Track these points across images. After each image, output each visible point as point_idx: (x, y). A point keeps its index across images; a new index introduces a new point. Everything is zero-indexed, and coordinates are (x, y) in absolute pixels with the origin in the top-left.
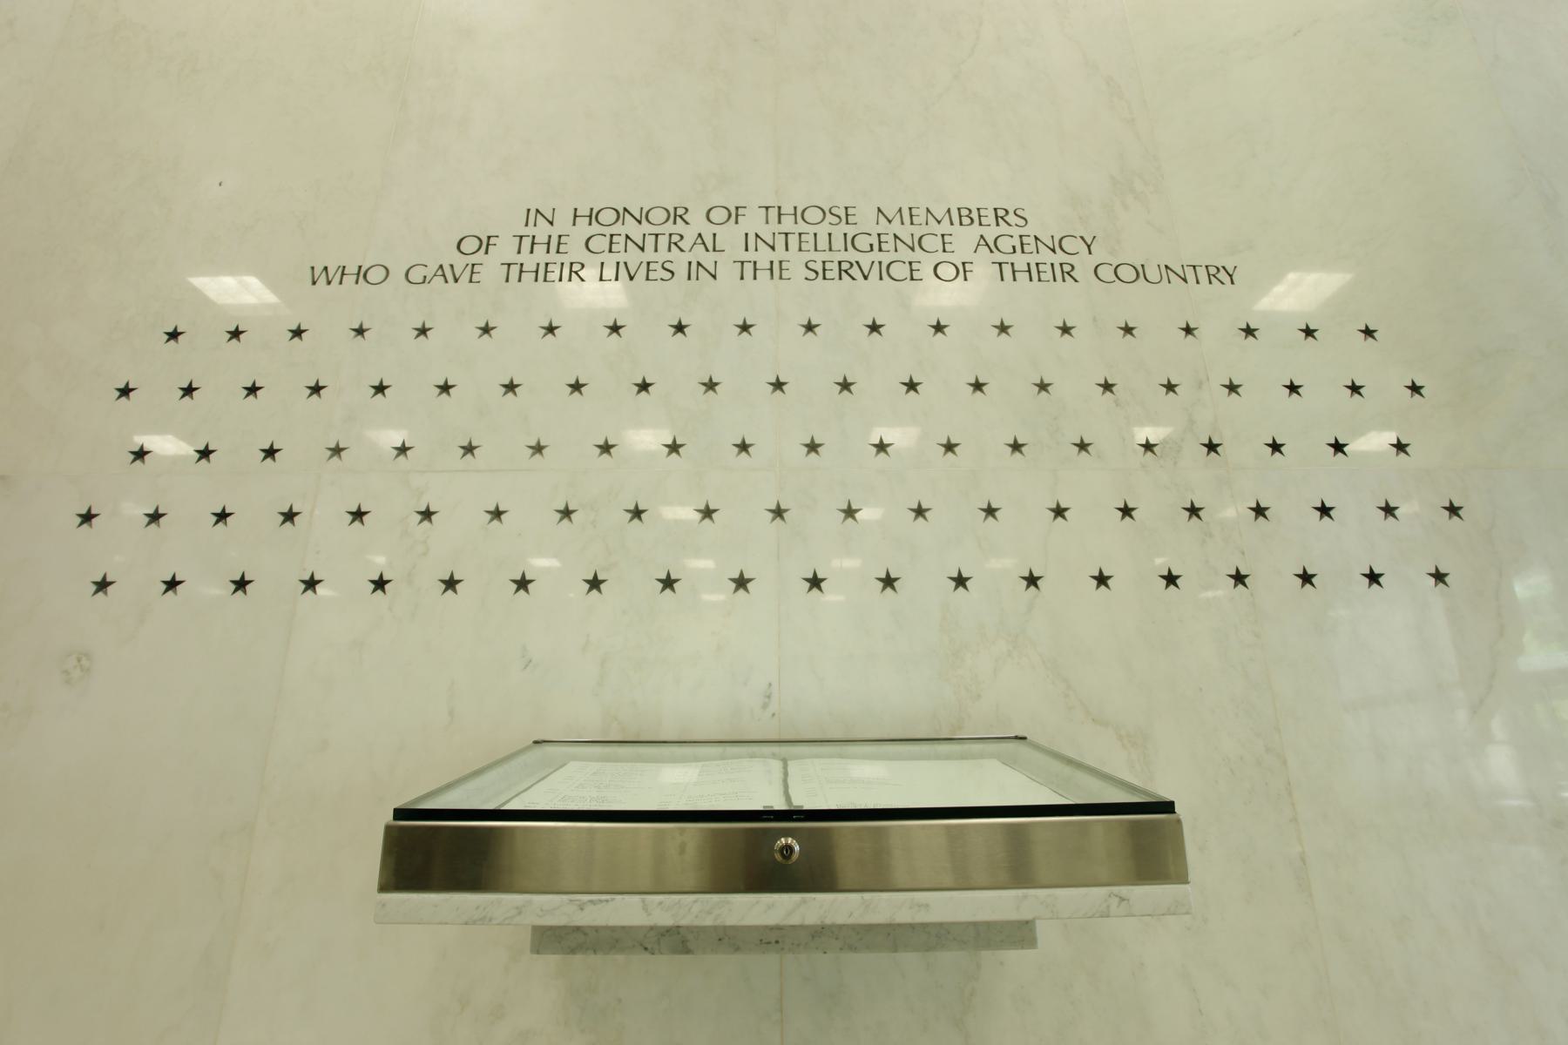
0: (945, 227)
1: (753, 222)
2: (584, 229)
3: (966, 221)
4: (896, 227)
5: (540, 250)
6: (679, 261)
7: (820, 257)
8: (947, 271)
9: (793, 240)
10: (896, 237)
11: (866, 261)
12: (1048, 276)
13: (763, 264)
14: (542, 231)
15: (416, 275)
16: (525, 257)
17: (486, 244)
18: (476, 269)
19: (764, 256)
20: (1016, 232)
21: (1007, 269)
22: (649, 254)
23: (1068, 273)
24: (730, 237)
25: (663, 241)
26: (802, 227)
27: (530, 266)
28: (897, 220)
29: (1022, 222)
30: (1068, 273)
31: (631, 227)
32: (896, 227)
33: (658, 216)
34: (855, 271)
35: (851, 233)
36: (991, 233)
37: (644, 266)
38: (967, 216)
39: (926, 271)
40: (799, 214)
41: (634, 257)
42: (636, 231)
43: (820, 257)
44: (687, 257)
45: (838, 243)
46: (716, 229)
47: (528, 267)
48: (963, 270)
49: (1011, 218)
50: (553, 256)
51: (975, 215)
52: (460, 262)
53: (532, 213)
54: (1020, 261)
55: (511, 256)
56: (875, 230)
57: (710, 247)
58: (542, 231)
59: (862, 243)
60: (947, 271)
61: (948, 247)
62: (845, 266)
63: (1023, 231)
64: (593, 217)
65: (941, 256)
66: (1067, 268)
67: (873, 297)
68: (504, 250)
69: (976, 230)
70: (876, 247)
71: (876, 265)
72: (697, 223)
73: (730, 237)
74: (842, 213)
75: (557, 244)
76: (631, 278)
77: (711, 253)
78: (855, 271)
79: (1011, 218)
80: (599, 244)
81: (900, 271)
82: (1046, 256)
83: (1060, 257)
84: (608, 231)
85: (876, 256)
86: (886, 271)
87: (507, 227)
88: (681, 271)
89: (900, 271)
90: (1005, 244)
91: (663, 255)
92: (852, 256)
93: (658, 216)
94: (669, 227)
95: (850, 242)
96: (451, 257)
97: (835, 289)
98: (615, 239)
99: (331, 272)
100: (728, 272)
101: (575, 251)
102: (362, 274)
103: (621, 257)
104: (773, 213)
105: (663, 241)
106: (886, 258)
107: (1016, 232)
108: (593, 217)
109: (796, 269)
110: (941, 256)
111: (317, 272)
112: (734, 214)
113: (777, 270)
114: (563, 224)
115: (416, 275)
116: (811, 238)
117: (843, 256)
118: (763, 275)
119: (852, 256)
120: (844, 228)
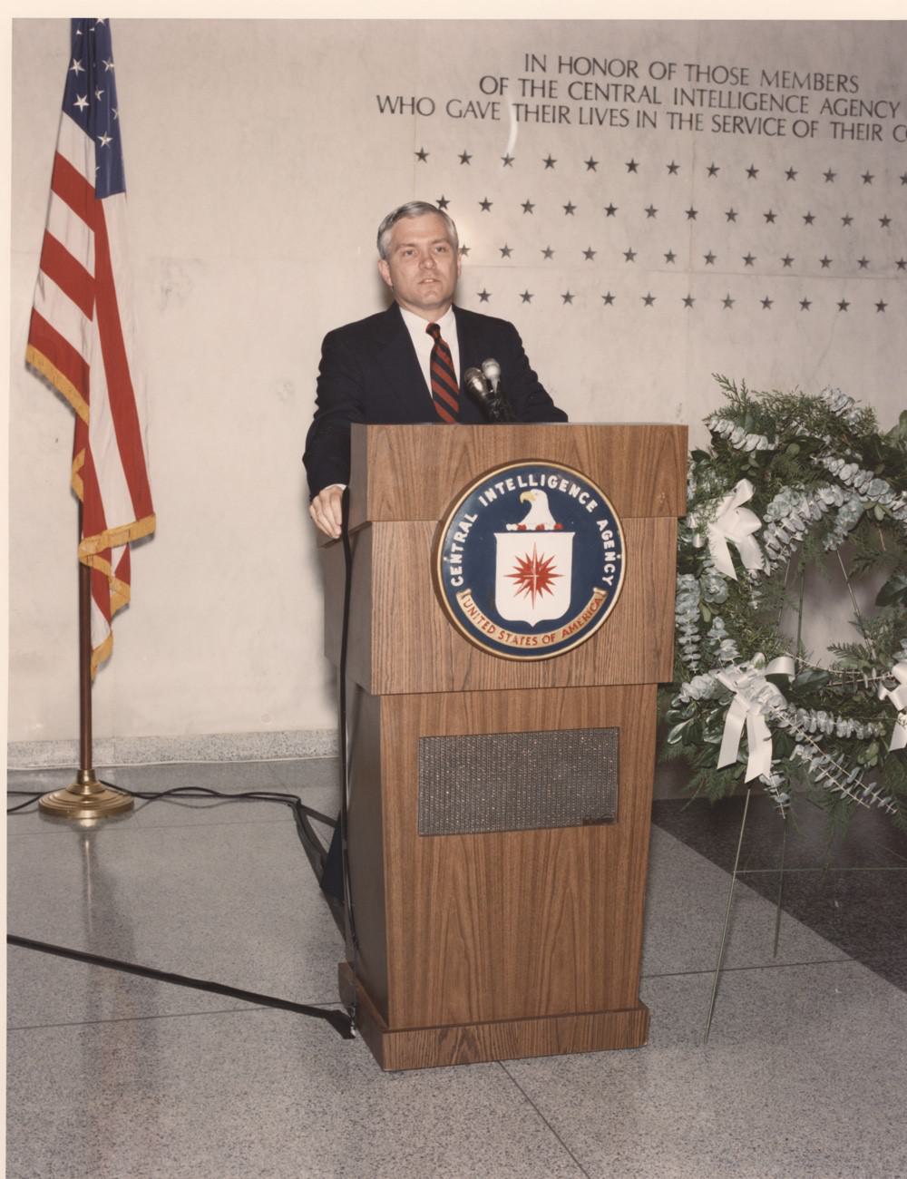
0: (804, 91)
1: (680, 80)
2: (566, 77)
3: (819, 85)
4: (773, 90)
5: (538, 92)
6: (632, 109)
7: (723, 112)
8: (801, 129)
9: (706, 95)
10: (772, 98)
11: (751, 116)
12: (863, 135)
13: (686, 117)
14: (538, 76)
15: (454, 109)
16: (527, 99)
17: (500, 86)
18: (496, 107)
19: (686, 109)
20: (849, 96)
21: (839, 128)
22: (612, 104)
23: (877, 133)
24: (665, 90)
25: (621, 90)
26: (713, 86)
27: (532, 108)
28: (774, 84)
29: (854, 88)
30: (877, 133)
32: (773, 90)
33: (617, 68)
34: (744, 126)
35: (744, 90)
36: (833, 97)
37: (609, 112)
38: (820, 81)
39: (787, 129)
40: (711, 74)
41: (602, 105)
43: (723, 112)
44: (637, 107)
45: (735, 102)
46: (656, 83)
47: (532, 108)
49: (849, 85)
50: (547, 101)
51: (825, 81)
52: (484, 100)
53: (530, 58)
54: (848, 121)
56: (759, 90)
57: (652, 98)
58: (538, 76)
59: (751, 101)
61: (805, 109)
62: (738, 121)
63: (853, 96)
64: (573, 65)
65: (799, 116)
66: (877, 129)
67: (753, 147)
68: (511, 95)
69: (824, 94)
70: (758, 107)
71: (757, 121)
72: (642, 80)
73: (665, 90)
74: (738, 73)
75: (548, 89)
76: (601, 123)
77: (653, 105)
78: (744, 126)
79: (849, 85)
81: (772, 127)
82: (867, 119)
83: (875, 120)
84: (584, 79)
85: (758, 114)
87: (514, 71)
88: (633, 119)
89: (772, 127)
90: (841, 107)
91: (620, 105)
92: (742, 112)
93: (617, 68)
94: (624, 80)
95: (743, 100)
96: (476, 95)
97: (731, 139)
98: (589, 87)
99: (393, 101)
100: (663, 121)
102: (415, 106)
103: (593, 104)
104: (694, 70)
105: (621, 90)
106: (764, 115)
107: (849, 96)
108: (573, 65)
109: (708, 124)
110: (799, 116)
111: (383, 100)
112: (668, 71)
113: (694, 122)
114: (552, 72)
115: (454, 109)
116: (716, 95)
117: (735, 112)
118: (686, 125)
119: (742, 112)
120: (740, 88)
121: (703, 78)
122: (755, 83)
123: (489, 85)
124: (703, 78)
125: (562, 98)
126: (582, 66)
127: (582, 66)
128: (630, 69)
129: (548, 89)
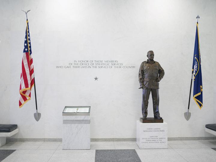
2: (79, 63)
8: (110, 67)
11: (103, 66)
14: (76, 63)
17: (71, 64)
31: (83, 63)
39: (108, 67)
42: (83, 63)
48: (111, 67)
55: (74, 65)
60: (110, 67)
80: (81, 64)
86: (105, 67)
100: (92, 67)
101: (79, 65)
108: (80, 61)
121: (97, 62)
122: (104, 62)
123: (70, 64)
124: (97, 62)
125: (79, 65)
126: (81, 61)
127: (81, 61)
128: (87, 61)
129: (77, 64)
